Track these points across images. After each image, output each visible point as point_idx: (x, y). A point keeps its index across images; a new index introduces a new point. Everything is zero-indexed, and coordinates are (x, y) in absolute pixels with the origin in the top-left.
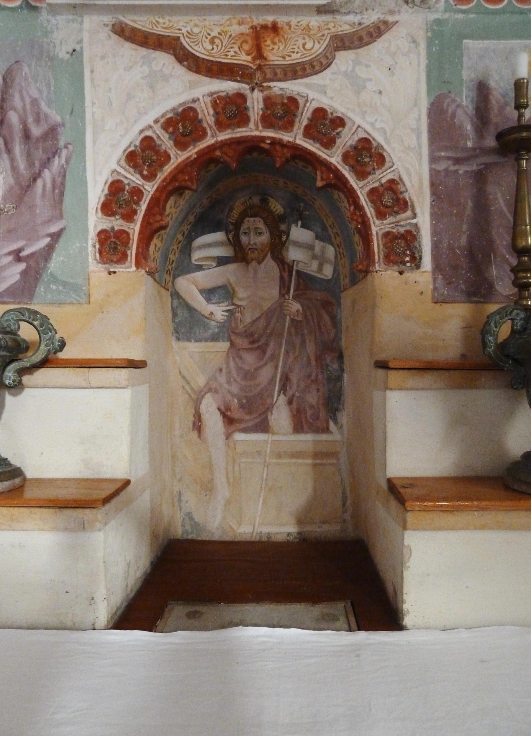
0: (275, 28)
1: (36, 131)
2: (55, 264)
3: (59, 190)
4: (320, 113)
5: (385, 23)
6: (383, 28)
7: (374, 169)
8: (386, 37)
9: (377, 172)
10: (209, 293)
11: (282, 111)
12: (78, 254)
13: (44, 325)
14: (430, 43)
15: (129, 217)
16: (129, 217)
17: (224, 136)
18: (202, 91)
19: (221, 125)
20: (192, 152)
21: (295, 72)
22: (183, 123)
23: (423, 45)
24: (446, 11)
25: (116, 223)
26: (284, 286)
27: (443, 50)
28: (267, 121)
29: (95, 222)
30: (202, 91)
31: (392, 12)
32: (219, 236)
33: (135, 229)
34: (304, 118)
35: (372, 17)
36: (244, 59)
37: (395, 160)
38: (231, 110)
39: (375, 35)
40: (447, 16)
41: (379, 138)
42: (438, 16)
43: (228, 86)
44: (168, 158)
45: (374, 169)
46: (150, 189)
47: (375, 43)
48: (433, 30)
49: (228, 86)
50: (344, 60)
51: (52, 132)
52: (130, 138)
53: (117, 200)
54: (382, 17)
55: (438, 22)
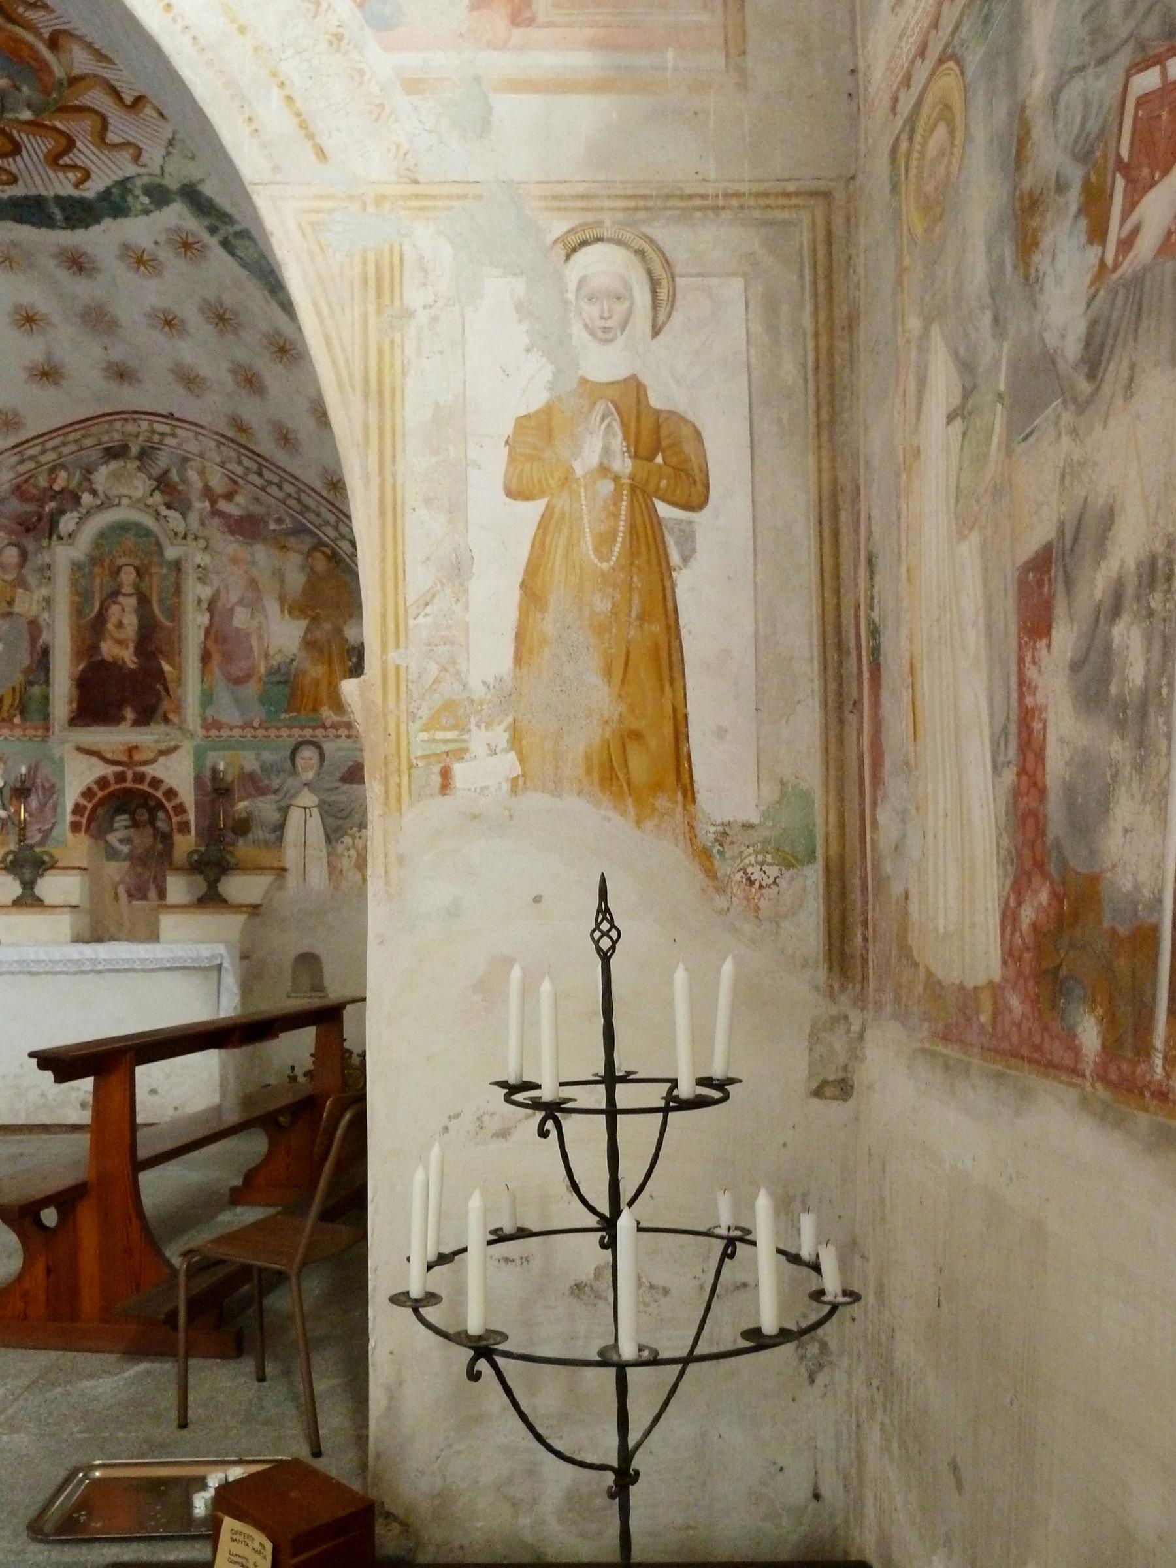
0: (136, 748)
1: (47, 785)
3: (55, 807)
4: (154, 778)
10: (121, 841)
11: (139, 778)
12: (63, 828)
13: (51, 856)
15: (82, 816)
16: (82, 816)
17: (118, 787)
18: (110, 770)
19: (116, 783)
20: (106, 792)
22: (102, 782)
25: (77, 818)
26: (155, 837)
27: (199, 755)
29: (69, 818)
30: (110, 770)
32: (126, 816)
33: (84, 821)
34: (148, 780)
35: (173, 744)
36: (125, 759)
38: (120, 777)
41: (175, 787)
43: (119, 768)
44: (96, 794)
46: (90, 806)
49: (119, 768)
50: (162, 759)
51: (53, 786)
52: (82, 788)
53: (78, 810)
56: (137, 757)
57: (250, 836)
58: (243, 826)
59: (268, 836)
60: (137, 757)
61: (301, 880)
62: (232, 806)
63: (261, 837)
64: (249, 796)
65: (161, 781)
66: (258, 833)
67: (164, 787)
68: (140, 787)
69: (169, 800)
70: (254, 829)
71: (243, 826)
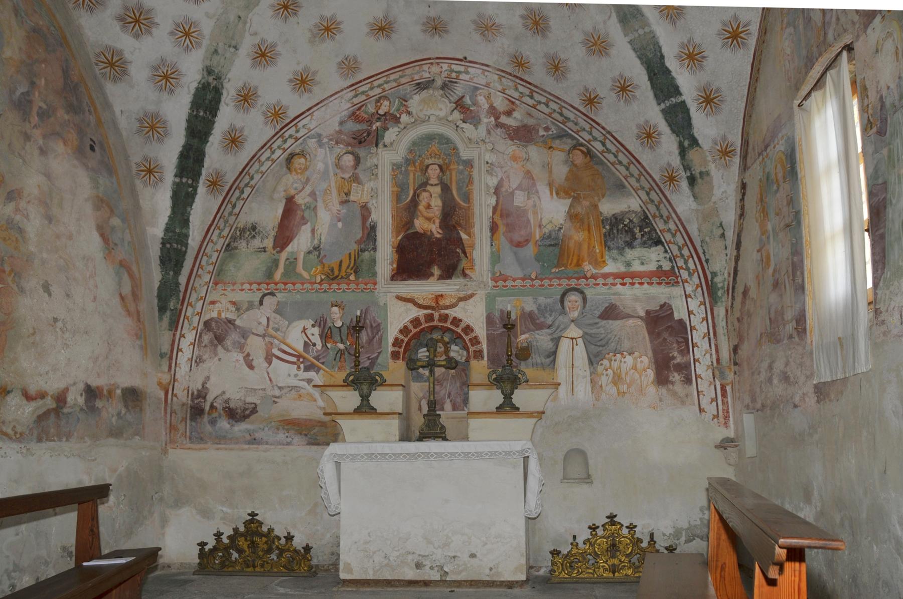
0: (442, 296)
2: (380, 360)
4: (455, 318)
11: (444, 318)
21: (447, 307)
28: (440, 321)
36: (433, 304)
56: (442, 303)
57: (530, 360)
58: (525, 353)
59: (543, 360)
60: (442, 303)
61: (570, 394)
62: (516, 337)
63: (539, 361)
64: (529, 330)
65: (461, 320)
66: (535, 358)
67: (462, 325)
68: (445, 325)
69: (467, 334)
70: (532, 355)
71: (525, 353)
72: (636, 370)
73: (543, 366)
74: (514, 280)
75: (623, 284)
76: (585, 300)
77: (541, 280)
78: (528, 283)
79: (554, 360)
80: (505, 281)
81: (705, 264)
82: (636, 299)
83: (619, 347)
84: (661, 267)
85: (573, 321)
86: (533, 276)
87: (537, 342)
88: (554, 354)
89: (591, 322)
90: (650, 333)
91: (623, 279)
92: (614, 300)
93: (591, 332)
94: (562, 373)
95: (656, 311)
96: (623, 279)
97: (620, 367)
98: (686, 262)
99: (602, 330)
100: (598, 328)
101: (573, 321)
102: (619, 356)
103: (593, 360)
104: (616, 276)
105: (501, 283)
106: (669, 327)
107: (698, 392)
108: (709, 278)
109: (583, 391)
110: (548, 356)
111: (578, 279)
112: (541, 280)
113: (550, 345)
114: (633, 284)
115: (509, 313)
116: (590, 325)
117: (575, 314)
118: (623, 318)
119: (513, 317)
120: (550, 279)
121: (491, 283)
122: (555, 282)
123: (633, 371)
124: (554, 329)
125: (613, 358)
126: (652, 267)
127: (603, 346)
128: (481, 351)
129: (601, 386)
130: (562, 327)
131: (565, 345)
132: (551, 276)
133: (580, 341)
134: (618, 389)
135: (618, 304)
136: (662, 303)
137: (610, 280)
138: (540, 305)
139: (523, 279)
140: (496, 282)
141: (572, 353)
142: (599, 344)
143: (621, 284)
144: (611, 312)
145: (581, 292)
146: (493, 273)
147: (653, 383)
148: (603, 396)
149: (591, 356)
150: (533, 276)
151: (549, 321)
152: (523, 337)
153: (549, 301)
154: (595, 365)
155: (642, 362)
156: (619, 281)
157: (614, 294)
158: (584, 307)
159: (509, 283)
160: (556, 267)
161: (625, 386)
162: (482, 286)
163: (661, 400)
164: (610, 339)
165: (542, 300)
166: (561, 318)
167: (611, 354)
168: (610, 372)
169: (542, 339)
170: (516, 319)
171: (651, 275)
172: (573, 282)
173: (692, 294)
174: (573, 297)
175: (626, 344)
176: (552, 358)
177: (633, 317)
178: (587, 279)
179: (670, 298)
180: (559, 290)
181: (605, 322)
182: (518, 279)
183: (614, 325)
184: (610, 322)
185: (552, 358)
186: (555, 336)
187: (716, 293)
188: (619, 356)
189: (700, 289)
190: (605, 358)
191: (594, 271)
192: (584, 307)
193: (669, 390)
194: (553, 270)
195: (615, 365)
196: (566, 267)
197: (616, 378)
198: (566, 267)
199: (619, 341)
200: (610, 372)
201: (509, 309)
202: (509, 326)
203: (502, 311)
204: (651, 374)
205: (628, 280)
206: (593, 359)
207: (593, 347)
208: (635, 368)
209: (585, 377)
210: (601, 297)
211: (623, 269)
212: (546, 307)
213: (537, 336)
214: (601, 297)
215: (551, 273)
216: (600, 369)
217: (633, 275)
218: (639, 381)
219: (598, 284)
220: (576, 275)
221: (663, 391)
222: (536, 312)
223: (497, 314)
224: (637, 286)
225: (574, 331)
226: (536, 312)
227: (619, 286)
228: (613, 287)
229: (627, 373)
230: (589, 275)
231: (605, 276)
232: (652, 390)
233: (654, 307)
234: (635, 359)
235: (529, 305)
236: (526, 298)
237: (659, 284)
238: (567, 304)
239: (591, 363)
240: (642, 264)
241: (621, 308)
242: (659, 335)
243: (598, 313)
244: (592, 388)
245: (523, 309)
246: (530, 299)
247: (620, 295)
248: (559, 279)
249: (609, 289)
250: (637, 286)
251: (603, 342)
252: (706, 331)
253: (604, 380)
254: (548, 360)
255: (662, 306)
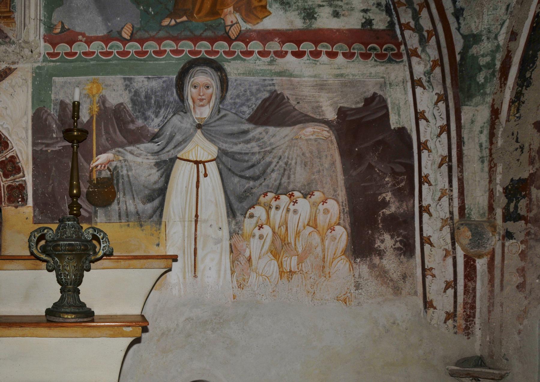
5: (10, 69)
6: (8, 72)
7: (2, 150)
8: (10, 77)
9: (5, 152)
14: (34, 79)
23: (30, 81)
24: (44, 61)
31: (14, 63)
37: (14, 145)
39: (4, 76)
40: (44, 64)
42: (39, 64)
45: (2, 150)
47: (4, 81)
48: (36, 73)
54: (8, 66)
55: (39, 68)
57: (115, 206)
58: (105, 192)
59: (141, 206)
61: (189, 275)
62: (89, 158)
63: (132, 208)
64: (115, 145)
66: (126, 202)
70: (120, 195)
71: (105, 192)
72: (315, 227)
73: (139, 219)
74: (89, 41)
75: (299, 54)
76: (224, 83)
77: (142, 42)
78: (116, 46)
79: (161, 206)
80: (71, 44)
81: (452, 20)
82: (322, 86)
83: (285, 180)
84: (369, 22)
85: (199, 126)
86: (126, 35)
87: (129, 169)
88: (159, 194)
89: (235, 128)
90: (346, 153)
91: (298, 44)
92: (280, 85)
93: (236, 149)
94: (175, 236)
95: (357, 111)
96: (298, 44)
97: (286, 223)
98: (416, 16)
99: (254, 147)
100: (248, 142)
101: (199, 126)
102: (284, 198)
103: (237, 206)
104: (286, 36)
105: (63, 48)
106: (379, 143)
107: (424, 269)
108: (459, 47)
109: (215, 265)
110: (150, 199)
111: (212, 41)
112: (142, 42)
113: (154, 176)
114: (316, 54)
115: (76, 106)
116: (232, 135)
117: (204, 112)
118: (294, 124)
119: (84, 117)
120: (159, 41)
121: (43, 47)
122: (169, 46)
123: (310, 229)
124: (162, 142)
125: (274, 204)
126: (353, 22)
127: (254, 178)
128: (22, 188)
129: (249, 260)
130: (179, 137)
131: (183, 174)
132: (162, 34)
133: (212, 167)
134: (281, 266)
135: (287, 93)
136: (369, 94)
137: (274, 46)
138: (136, 93)
139: (106, 40)
140: (54, 45)
141: (196, 191)
142: (248, 173)
143: (295, 54)
144: (274, 111)
145: (218, 68)
146: (50, 27)
147: (344, 252)
148: (253, 278)
149: (232, 198)
150: (126, 35)
151: (154, 126)
152: (103, 158)
153: (155, 84)
154: (240, 218)
155: (326, 211)
156: (289, 47)
157: (281, 74)
158: (222, 98)
159: (80, 48)
160: (173, 15)
161: (295, 260)
162: (27, 52)
163: (358, 286)
164: (270, 163)
165: (141, 82)
166: (176, 120)
167: (271, 195)
168: (267, 230)
169: (138, 163)
170: (90, 122)
171: (350, 37)
172: (203, 47)
173: (424, 79)
174: (202, 78)
175: (300, 176)
176: (156, 202)
177: (314, 120)
178: (229, 41)
179: (383, 85)
180: (177, 63)
181: (260, 129)
182: (97, 39)
183: (279, 136)
184: (272, 129)
185: (156, 202)
186: (165, 156)
187: (473, 78)
188: (284, 198)
189: (438, 70)
190: (258, 203)
191: (245, 26)
192: (222, 98)
193: (372, 267)
194: (166, 22)
195: (277, 216)
196: (190, 16)
197: (278, 243)
198: (190, 16)
199: (287, 169)
200: (267, 230)
201: (77, 98)
202: (76, 135)
203: (62, 104)
204: (342, 235)
205: (307, 47)
206: (236, 205)
207: (236, 180)
208: (313, 223)
209: (219, 241)
210: (256, 79)
211: (298, 24)
212: (148, 97)
213: (129, 157)
214: (256, 79)
215: (161, 28)
216: (248, 224)
217: (319, 37)
218: (319, 249)
219: (251, 53)
220: (209, 34)
221: (364, 269)
222: (129, 106)
223: (53, 111)
224: (324, 58)
225: (201, 148)
226: (129, 106)
227: (289, 57)
228: (280, 60)
229: (298, 234)
230: (233, 33)
231: (265, 36)
232: (342, 266)
233: (353, 101)
234: (314, 205)
235: (116, 94)
236: (109, 79)
237: (365, 56)
238: (190, 91)
239: (231, 212)
240: (336, 14)
241: (293, 102)
242: (360, 157)
243: (248, 111)
244: (233, 262)
245: (103, 101)
246: (117, 80)
247: (291, 75)
248: (176, 40)
249: (271, 63)
250: (324, 58)
251: (257, 171)
252: (446, 153)
253: (255, 248)
254: (149, 207)
255: (368, 101)
